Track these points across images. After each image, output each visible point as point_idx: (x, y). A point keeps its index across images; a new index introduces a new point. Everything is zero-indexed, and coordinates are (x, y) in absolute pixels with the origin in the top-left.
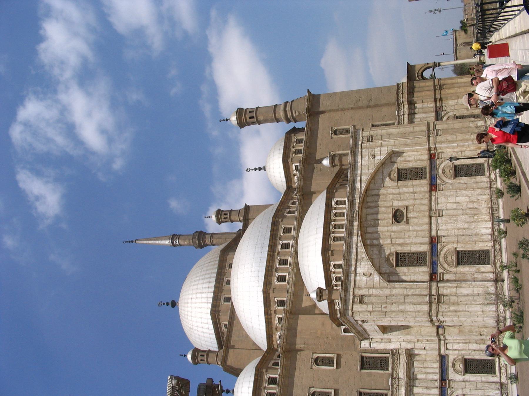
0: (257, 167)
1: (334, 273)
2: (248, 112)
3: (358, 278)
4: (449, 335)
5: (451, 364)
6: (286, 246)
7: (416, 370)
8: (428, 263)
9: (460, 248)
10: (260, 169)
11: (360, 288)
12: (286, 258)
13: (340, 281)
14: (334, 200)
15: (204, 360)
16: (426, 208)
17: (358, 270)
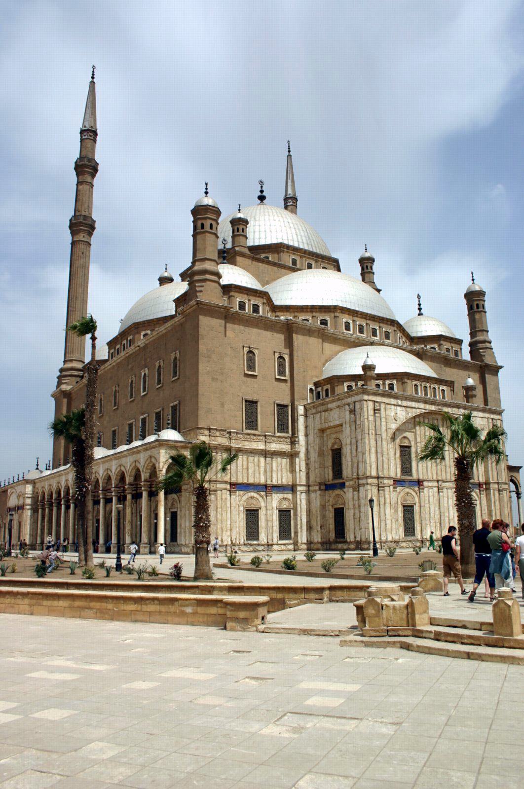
0: (422, 306)
1: (384, 384)
2: (483, 303)
3: (393, 407)
4: (320, 495)
5: (285, 496)
6: (374, 333)
7: (279, 459)
8: (404, 477)
9: (416, 508)
10: (420, 309)
11: (385, 409)
12: (365, 332)
13: (389, 389)
14: (445, 388)
15: (238, 231)
16: (444, 478)
17: (399, 408)
